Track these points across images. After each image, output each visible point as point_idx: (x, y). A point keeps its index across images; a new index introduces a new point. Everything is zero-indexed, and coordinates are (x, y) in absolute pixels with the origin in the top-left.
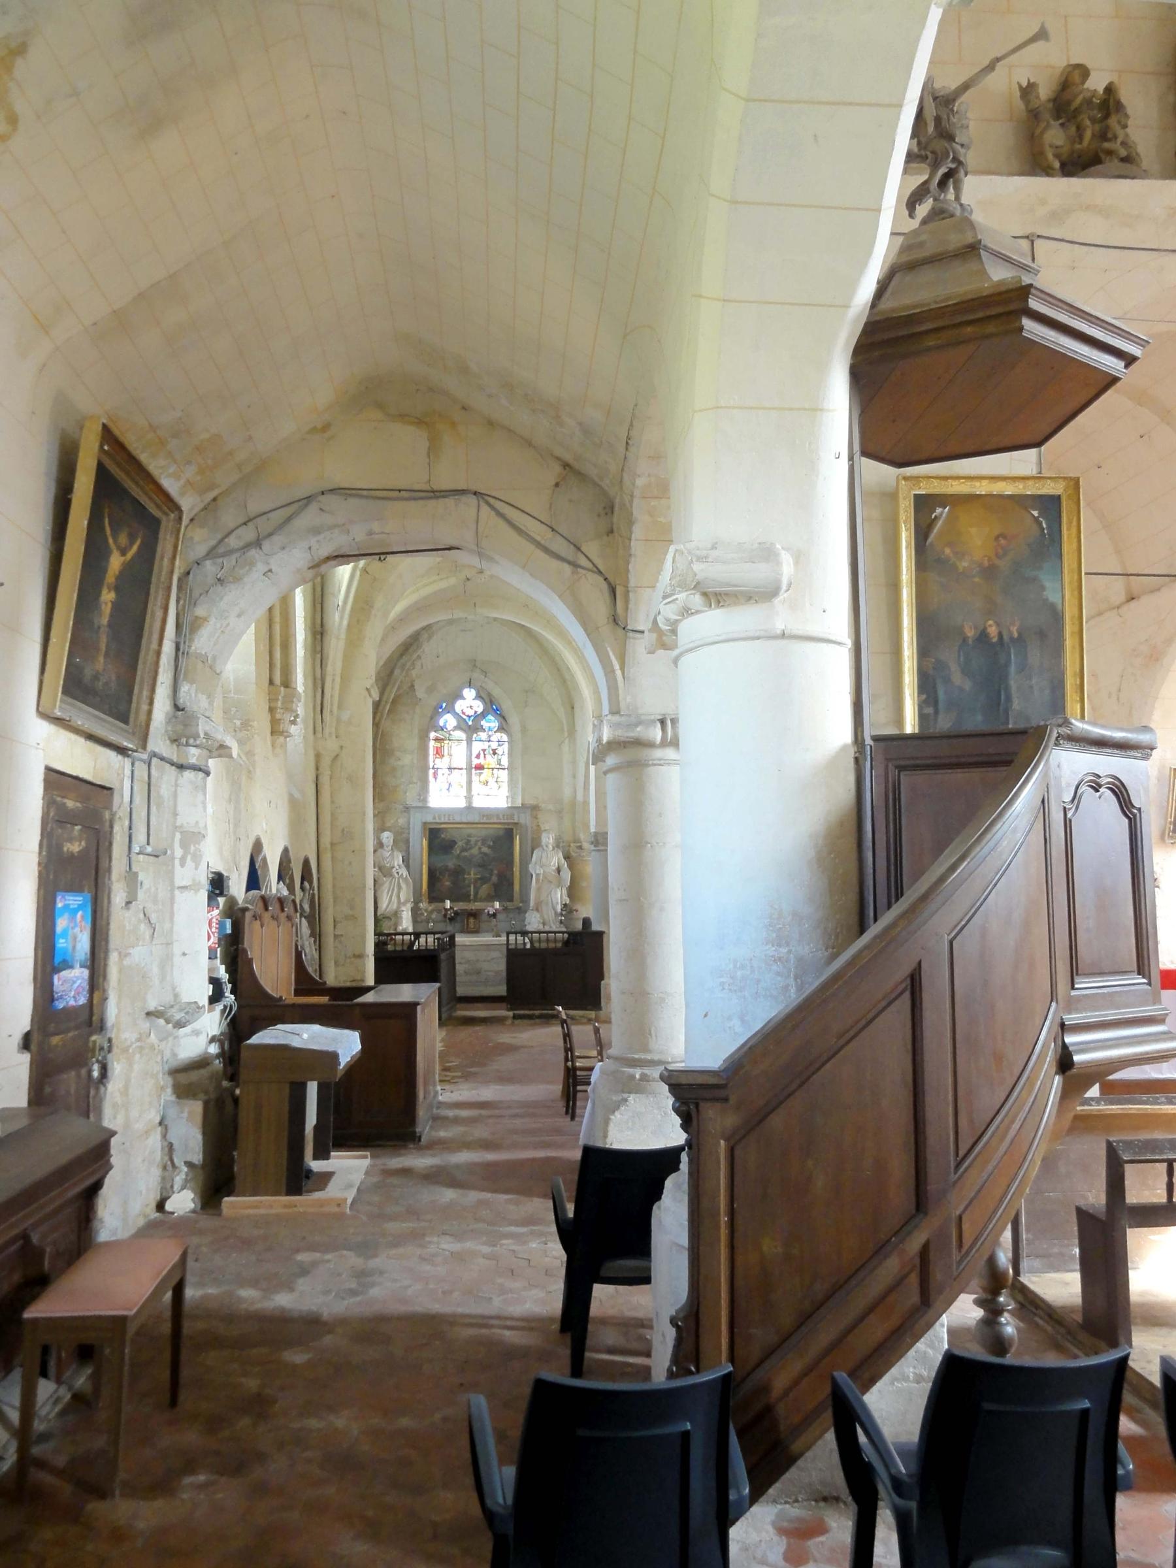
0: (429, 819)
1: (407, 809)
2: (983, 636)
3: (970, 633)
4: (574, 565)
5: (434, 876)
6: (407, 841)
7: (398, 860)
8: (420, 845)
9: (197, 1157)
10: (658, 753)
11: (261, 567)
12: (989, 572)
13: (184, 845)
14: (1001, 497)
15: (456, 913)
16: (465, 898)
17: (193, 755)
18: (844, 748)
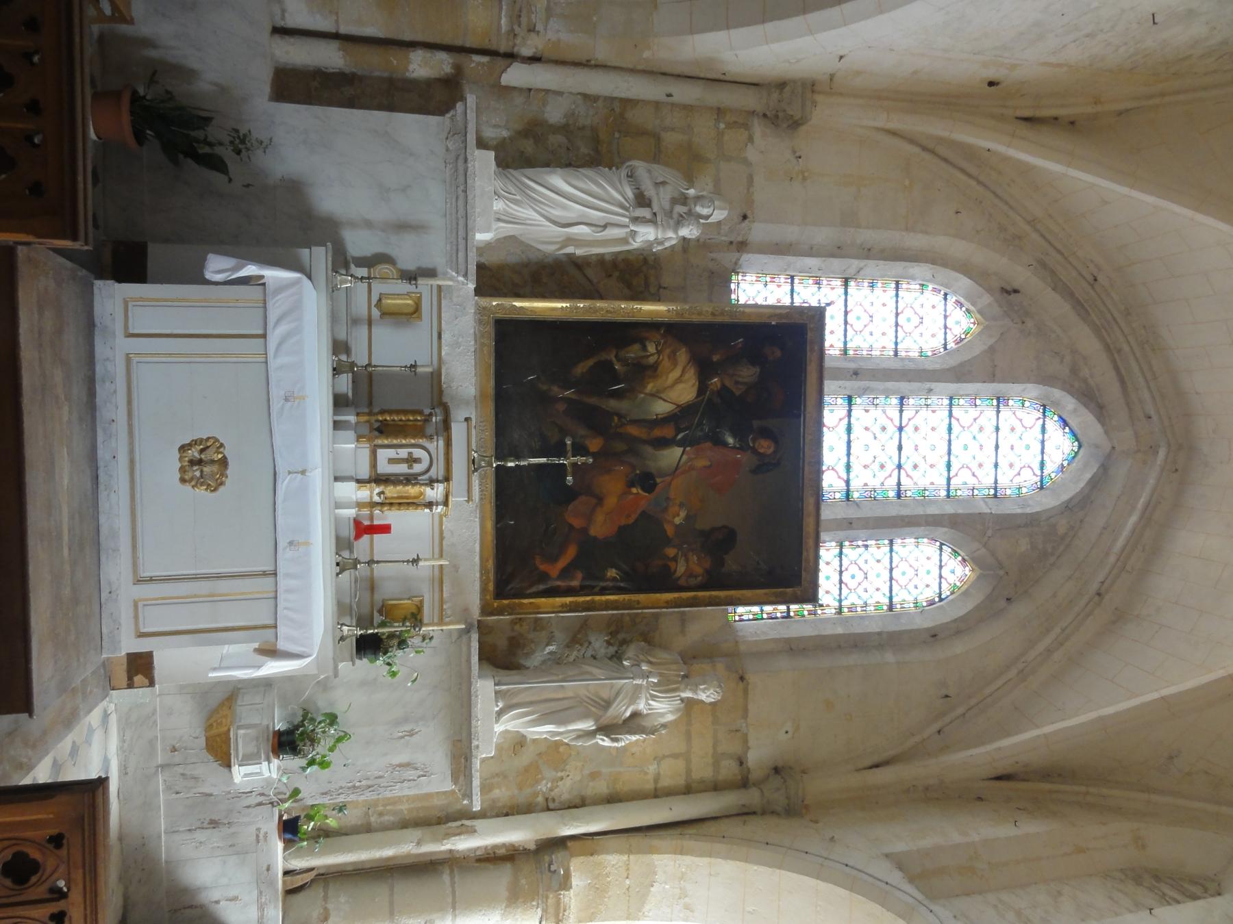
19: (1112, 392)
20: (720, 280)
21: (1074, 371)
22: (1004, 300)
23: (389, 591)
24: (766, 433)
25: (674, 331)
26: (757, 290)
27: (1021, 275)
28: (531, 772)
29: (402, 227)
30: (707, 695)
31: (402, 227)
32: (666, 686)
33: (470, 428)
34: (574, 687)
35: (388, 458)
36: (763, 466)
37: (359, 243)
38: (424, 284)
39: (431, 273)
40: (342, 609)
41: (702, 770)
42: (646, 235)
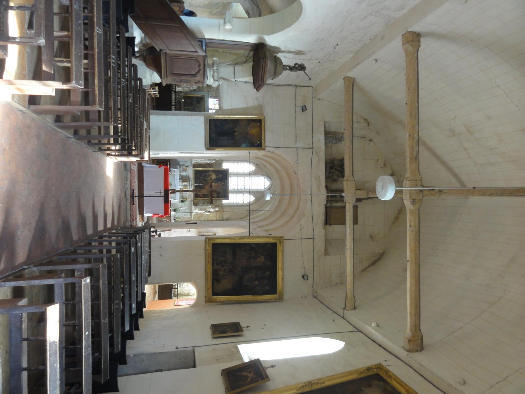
0: (206, 97)
1: (208, 92)
2: (235, 132)
4: (247, 57)
6: (200, 91)
7: (195, 88)
8: (199, 94)
10: (212, 70)
14: (261, 136)
15: (180, 103)
16: (185, 105)
18: (204, 36)
21: (267, 174)
22: (257, 165)
23: (184, 197)
25: (213, 171)
26: (225, 166)
27: (258, 163)
28: (199, 217)
29: (186, 162)
30: (217, 209)
31: (186, 162)
32: (212, 208)
33: (192, 181)
34: (202, 207)
35: (184, 184)
36: (223, 185)
37: (181, 163)
38: (188, 168)
39: (188, 166)
40: (180, 198)
41: (218, 219)
42: (209, 162)
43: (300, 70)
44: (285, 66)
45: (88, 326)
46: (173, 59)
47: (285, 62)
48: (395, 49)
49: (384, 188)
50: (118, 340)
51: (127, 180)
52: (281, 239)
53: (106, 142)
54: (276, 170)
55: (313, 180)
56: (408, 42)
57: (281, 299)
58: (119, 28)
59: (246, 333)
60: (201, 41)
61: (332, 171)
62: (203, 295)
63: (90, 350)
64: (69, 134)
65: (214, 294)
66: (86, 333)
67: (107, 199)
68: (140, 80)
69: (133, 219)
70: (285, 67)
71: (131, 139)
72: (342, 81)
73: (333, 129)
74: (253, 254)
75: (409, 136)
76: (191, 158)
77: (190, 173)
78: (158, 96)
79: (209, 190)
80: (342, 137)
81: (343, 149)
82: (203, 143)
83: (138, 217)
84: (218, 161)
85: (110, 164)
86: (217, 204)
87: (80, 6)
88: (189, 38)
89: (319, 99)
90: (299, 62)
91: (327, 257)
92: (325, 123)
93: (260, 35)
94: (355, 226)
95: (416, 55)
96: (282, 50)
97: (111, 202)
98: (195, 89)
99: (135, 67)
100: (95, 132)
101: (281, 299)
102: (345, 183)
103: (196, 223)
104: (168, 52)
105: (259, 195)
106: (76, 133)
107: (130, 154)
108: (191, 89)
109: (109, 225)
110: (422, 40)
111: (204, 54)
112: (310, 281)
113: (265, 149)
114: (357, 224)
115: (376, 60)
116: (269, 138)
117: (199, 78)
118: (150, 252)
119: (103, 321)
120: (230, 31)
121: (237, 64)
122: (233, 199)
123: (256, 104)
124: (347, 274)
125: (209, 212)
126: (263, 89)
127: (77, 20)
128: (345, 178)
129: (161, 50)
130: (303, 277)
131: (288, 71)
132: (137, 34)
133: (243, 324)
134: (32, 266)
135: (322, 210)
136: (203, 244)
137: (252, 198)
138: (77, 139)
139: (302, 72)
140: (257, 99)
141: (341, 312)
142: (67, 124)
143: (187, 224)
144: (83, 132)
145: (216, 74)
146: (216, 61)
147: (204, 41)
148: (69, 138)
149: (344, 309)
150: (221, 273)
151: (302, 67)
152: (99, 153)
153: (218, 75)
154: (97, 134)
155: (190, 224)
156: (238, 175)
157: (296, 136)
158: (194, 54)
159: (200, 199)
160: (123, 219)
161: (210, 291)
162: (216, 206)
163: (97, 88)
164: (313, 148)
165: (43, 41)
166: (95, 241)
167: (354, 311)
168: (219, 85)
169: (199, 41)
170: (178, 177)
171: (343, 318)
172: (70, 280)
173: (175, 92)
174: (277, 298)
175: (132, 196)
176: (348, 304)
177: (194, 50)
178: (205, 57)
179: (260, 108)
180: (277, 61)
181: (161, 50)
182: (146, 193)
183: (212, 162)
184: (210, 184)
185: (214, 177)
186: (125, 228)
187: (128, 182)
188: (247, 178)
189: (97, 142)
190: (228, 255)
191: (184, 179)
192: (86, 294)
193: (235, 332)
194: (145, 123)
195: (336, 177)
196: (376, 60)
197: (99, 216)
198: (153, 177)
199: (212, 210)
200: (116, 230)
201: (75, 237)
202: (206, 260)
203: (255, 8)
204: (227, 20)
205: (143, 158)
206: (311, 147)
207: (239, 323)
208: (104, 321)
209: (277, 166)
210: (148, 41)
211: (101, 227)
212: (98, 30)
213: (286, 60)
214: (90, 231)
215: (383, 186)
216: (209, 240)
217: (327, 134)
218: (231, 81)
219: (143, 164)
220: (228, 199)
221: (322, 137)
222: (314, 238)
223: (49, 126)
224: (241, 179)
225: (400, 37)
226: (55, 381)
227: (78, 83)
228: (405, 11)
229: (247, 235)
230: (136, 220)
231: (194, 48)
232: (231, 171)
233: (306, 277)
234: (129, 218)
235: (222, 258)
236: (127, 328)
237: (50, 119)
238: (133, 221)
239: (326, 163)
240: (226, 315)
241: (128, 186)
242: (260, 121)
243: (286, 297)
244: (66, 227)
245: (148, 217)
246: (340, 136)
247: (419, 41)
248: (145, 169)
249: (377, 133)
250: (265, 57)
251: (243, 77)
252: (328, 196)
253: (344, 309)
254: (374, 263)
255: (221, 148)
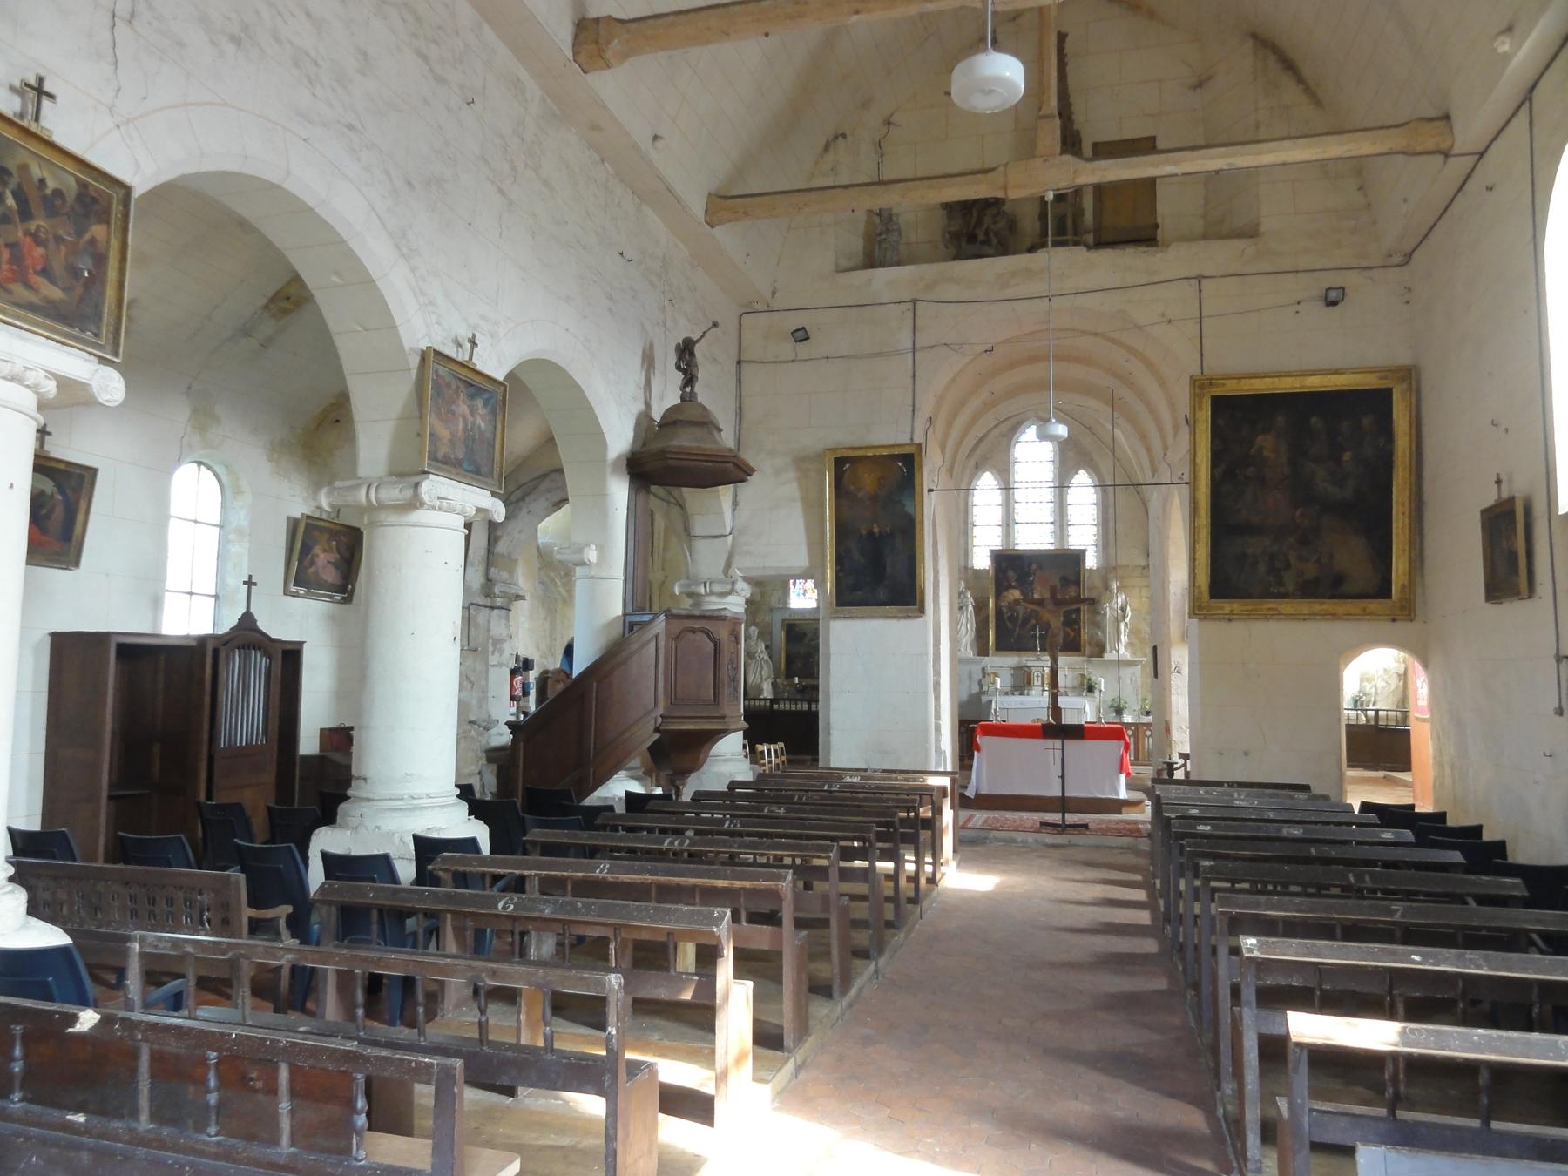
0: (787, 616)
2: (871, 533)
3: (864, 532)
5: (790, 660)
8: (779, 636)
9: (494, 790)
11: (525, 510)
12: (874, 498)
13: (494, 645)
17: (499, 602)
19: (1013, 421)
20: (978, 574)
22: (979, 467)
23: (1076, 683)
24: (1030, 565)
27: (972, 463)
29: (970, 676)
31: (970, 676)
33: (1028, 659)
34: (1109, 629)
36: (1040, 567)
37: (976, 689)
38: (989, 670)
40: (1080, 695)
43: (692, 354)
44: (683, 399)
45: (1393, 953)
46: (676, 700)
47: (673, 399)
48: (618, 88)
49: (988, 87)
50: (1486, 882)
51: (1014, 841)
52: (1199, 384)
53: (891, 884)
54: (988, 406)
55: (1009, 293)
56: (600, 54)
57: (1409, 374)
58: (603, 827)
59: (1518, 487)
60: (630, 626)
61: (981, 237)
62: (1387, 627)
63: (1470, 954)
64: (865, 974)
65: (1384, 591)
66: (1417, 959)
67: (1060, 895)
68: (733, 785)
69: (1132, 830)
70: (688, 398)
71: (893, 815)
72: (718, 231)
73: (857, 244)
74: (1250, 471)
75: (857, 12)
76: (956, 661)
77: (1001, 664)
78: (782, 745)
79: (1050, 607)
80: (880, 215)
81: (916, 207)
82: (903, 623)
83: (1129, 815)
84: (967, 582)
85: (960, 879)
86: (1098, 583)
87: (547, 901)
88: (624, 654)
89: (774, 293)
90: (672, 358)
91: (1263, 229)
92: (840, 270)
93: (609, 470)
94: (1160, 145)
95: (633, 26)
96: (641, 407)
97: (1071, 885)
98: (767, 647)
99: (699, 796)
100: (861, 911)
101: (1409, 374)
102: (1013, 194)
103: (1155, 648)
104: (660, 711)
105: (1070, 458)
106: (864, 954)
107: (932, 825)
108: (766, 657)
109: (1141, 895)
110: (593, 13)
111: (663, 617)
112: (1351, 280)
113: (919, 445)
114: (1153, 139)
115: (656, 138)
116: (888, 434)
117: (723, 634)
118: (1231, 785)
119: (1397, 917)
120: (601, 549)
121: (687, 529)
122: (1084, 536)
123: (791, 474)
124: (1320, 157)
125: (1123, 609)
126: (749, 457)
127: (576, 911)
128: (1000, 194)
129: (657, 730)
130: (1334, 303)
131: (697, 389)
132: (619, 788)
133: (1490, 498)
134: (1219, 1094)
135: (1106, 259)
136: (1211, 626)
137: (1082, 477)
138: (881, 951)
139: (698, 349)
140: (777, 472)
141: (1457, 167)
142: (836, 971)
143: (1156, 675)
144: (862, 938)
145: (717, 588)
146: (683, 586)
147: (629, 619)
148: (876, 971)
149: (1446, 154)
150: (1310, 570)
151: (686, 351)
152: (925, 904)
153: (720, 582)
154: (865, 904)
155: (1157, 668)
156: (1008, 523)
157: (879, 354)
158: (662, 643)
159: (1085, 636)
160: (1131, 859)
161: (1373, 605)
162: (1107, 588)
163: (738, 884)
164: (914, 301)
165: (613, 976)
166: (1176, 934)
167: (1453, 118)
168: (745, 579)
169: (631, 629)
170: (1016, 700)
171: (1482, 154)
172: (1249, 994)
173: (772, 701)
174: (1405, 386)
175: (1062, 828)
176: (1430, 145)
177: (653, 644)
178: (670, 616)
179: (803, 463)
180: (672, 420)
181: (657, 730)
182: (1056, 792)
183: (971, 599)
184: (1037, 604)
185: (1015, 594)
186: (1151, 855)
187: (1019, 836)
188: (1018, 495)
189: (890, 907)
190: (1250, 551)
191: (1022, 682)
192: (1291, 951)
193: (1513, 521)
194: (848, 779)
195: (1002, 224)
196: (656, 138)
197: (1107, 920)
198: (1009, 768)
199: (1121, 599)
200: (1154, 876)
201: (1161, 984)
202: (1266, 617)
203: (545, 484)
204: (576, 558)
205: (943, 790)
206: (910, 305)
207: (1485, 513)
208: (1399, 911)
209: (975, 403)
210: (636, 762)
211: (1144, 918)
212: (602, 870)
213: (667, 395)
214: (1150, 946)
215: (983, 91)
216: (1200, 608)
217: (871, 261)
218: (733, 546)
219: (970, 793)
220: (1084, 551)
221: (880, 273)
222: (1200, 278)
223: (843, 1014)
224: (1020, 513)
225: (589, 77)
226: (1528, 1043)
227: (717, 922)
228: (523, 74)
229: (1185, 489)
230: (1135, 822)
231: (646, 644)
232: (997, 544)
233: (1333, 295)
234: (1126, 841)
235: (1262, 568)
236: (1456, 857)
237: (820, 1009)
238: (1139, 830)
239: (958, 256)
240: (1458, 552)
241: (1031, 838)
242: (839, 463)
243: (1404, 358)
244: (1128, 1004)
245: (1130, 787)
246: (877, 220)
247: (597, 20)
248: (984, 791)
249: (865, 105)
250: (662, 454)
251: (721, 513)
252: (1056, 244)
253: (1446, 154)
254: (1289, 66)
255: (919, 571)
